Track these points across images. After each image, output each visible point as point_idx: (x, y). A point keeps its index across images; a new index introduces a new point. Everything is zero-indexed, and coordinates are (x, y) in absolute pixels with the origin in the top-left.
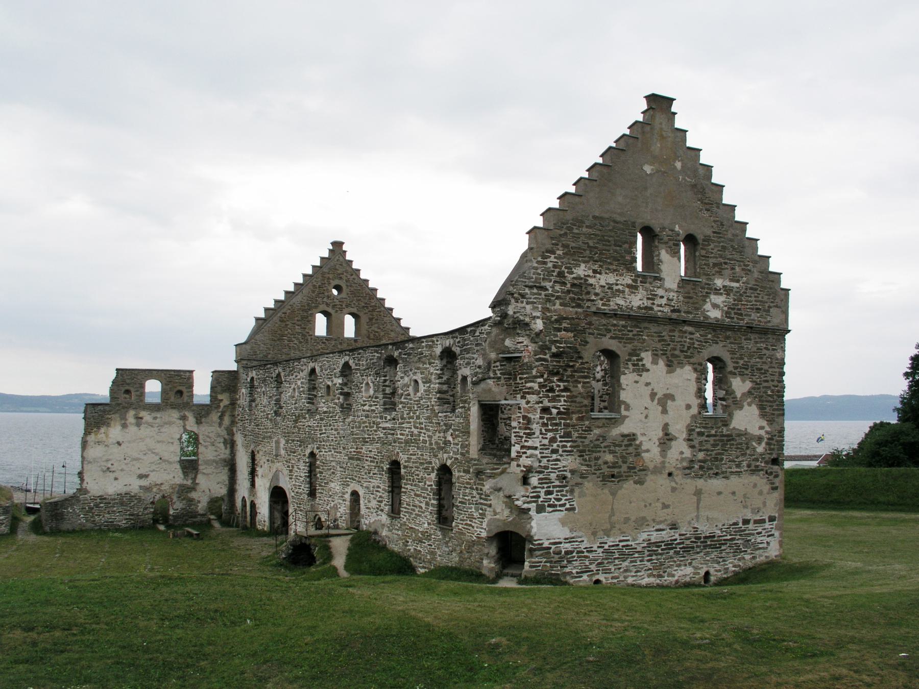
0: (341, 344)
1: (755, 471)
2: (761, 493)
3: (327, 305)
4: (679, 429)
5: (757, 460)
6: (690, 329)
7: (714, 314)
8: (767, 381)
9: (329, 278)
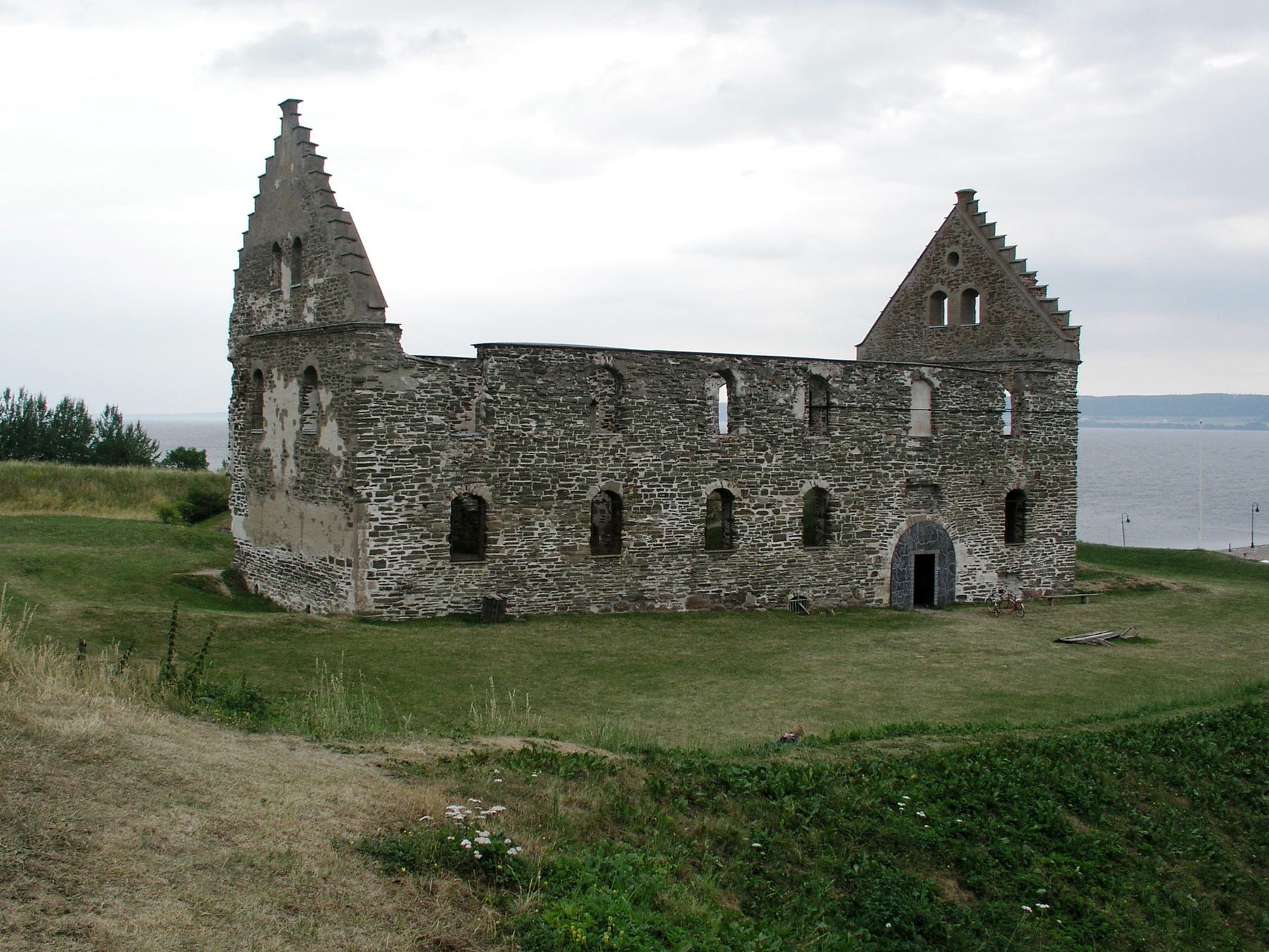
0: (957, 334)
1: (336, 499)
2: (340, 528)
3: (943, 282)
4: (290, 445)
5: (336, 486)
6: (295, 339)
7: (310, 319)
8: (343, 390)
9: (944, 246)
